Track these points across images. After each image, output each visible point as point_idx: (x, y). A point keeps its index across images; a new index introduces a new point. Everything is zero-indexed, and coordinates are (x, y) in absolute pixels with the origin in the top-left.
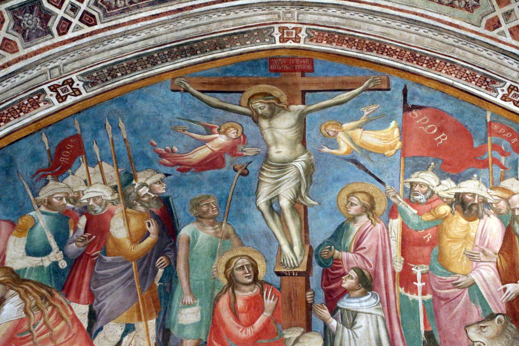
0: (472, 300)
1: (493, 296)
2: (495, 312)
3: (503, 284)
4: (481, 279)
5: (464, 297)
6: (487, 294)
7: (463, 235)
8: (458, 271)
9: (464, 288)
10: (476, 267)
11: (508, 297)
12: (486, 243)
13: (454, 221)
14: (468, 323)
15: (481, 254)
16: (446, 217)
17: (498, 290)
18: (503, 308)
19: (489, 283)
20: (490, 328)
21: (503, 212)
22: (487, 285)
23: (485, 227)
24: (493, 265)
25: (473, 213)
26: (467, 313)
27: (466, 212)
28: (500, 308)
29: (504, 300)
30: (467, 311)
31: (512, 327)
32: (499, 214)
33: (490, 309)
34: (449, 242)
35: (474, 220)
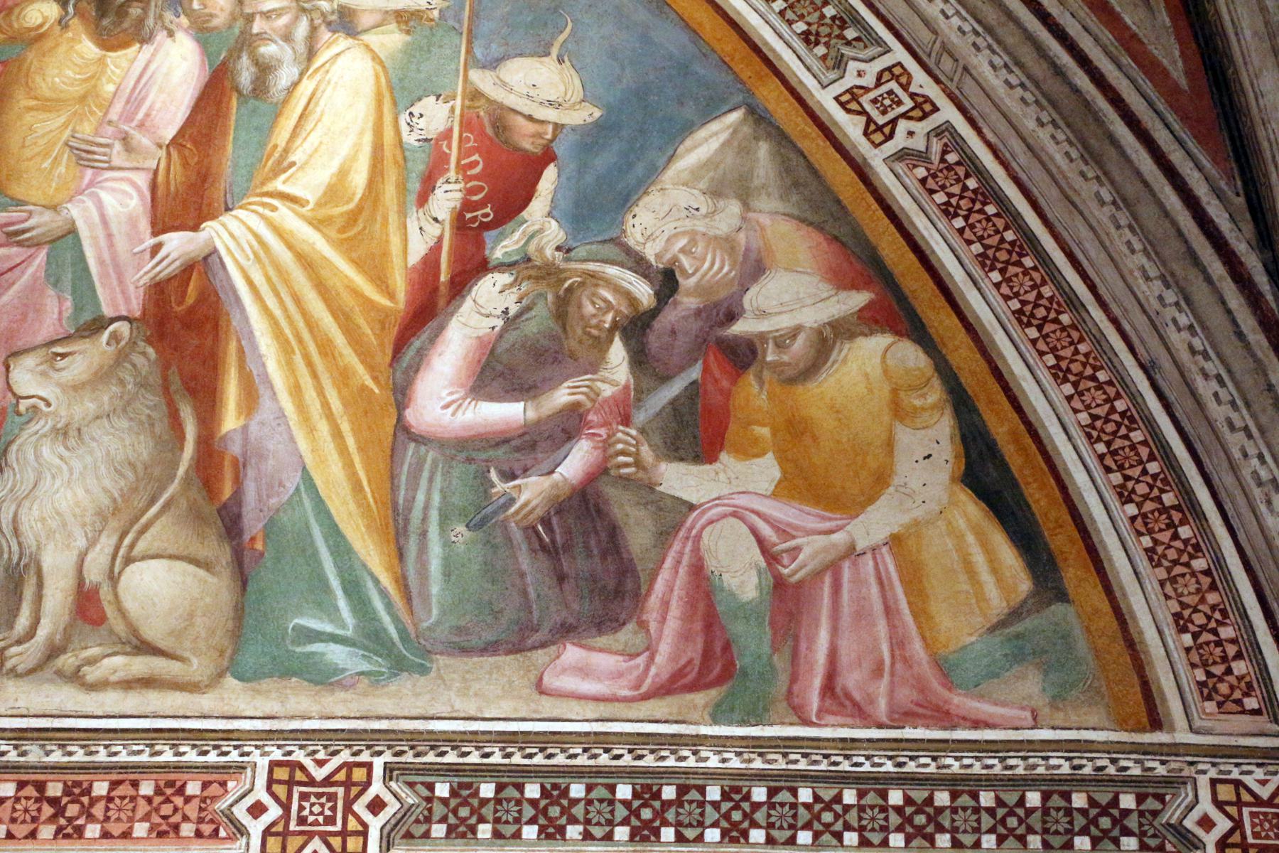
0: (52, 279)
1: (117, 266)
2: (108, 311)
3: (155, 234)
4: (96, 218)
5: (30, 271)
6: (101, 263)
7: (78, 90)
8: (35, 195)
9: (38, 245)
10: (91, 184)
11: (158, 269)
12: (140, 116)
13: (62, 49)
14: (20, 344)
15: (118, 146)
16: (41, 37)
17: (136, 250)
18: (134, 302)
19: (114, 228)
20: (78, 358)
21: (216, 22)
22: (110, 236)
23: (152, 67)
24: (142, 180)
25: (126, 25)
26: (24, 316)
27: (105, 22)
28: (127, 300)
29: (146, 279)
30: (29, 308)
31: (144, 354)
32: (202, 31)
33: (97, 304)
34: (30, 109)
35: (125, 45)
